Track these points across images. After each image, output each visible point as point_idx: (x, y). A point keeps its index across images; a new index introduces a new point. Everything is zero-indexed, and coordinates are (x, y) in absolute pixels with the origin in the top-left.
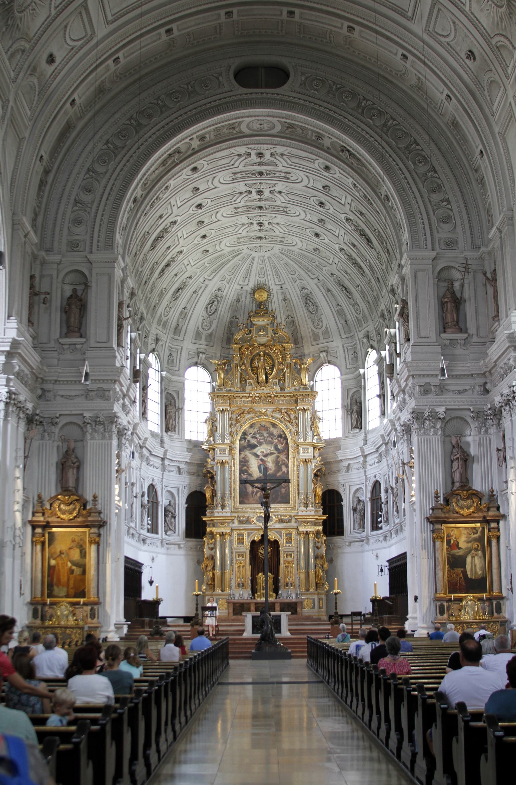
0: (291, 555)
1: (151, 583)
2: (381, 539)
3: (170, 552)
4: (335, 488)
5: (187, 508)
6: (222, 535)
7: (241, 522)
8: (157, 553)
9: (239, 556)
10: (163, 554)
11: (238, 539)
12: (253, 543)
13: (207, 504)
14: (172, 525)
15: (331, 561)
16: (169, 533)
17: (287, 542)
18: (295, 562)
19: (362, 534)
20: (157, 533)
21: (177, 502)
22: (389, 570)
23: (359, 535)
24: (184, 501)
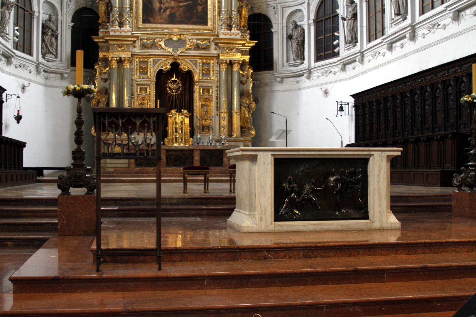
0: (208, 91)
1: (18, 118)
2: (337, 69)
3: (49, 82)
4: (262, 12)
5: (72, 27)
6: (120, 61)
7: (144, 46)
8: (28, 80)
9: (141, 89)
10: (39, 84)
11: (141, 68)
12: (160, 74)
13: (100, 21)
14: (52, 47)
15: (256, 100)
16: (48, 56)
17: (203, 74)
18: (214, 99)
19: (300, 67)
20: (31, 54)
21: (60, 18)
22: (356, 107)
23: (294, 69)
24: (70, 19)
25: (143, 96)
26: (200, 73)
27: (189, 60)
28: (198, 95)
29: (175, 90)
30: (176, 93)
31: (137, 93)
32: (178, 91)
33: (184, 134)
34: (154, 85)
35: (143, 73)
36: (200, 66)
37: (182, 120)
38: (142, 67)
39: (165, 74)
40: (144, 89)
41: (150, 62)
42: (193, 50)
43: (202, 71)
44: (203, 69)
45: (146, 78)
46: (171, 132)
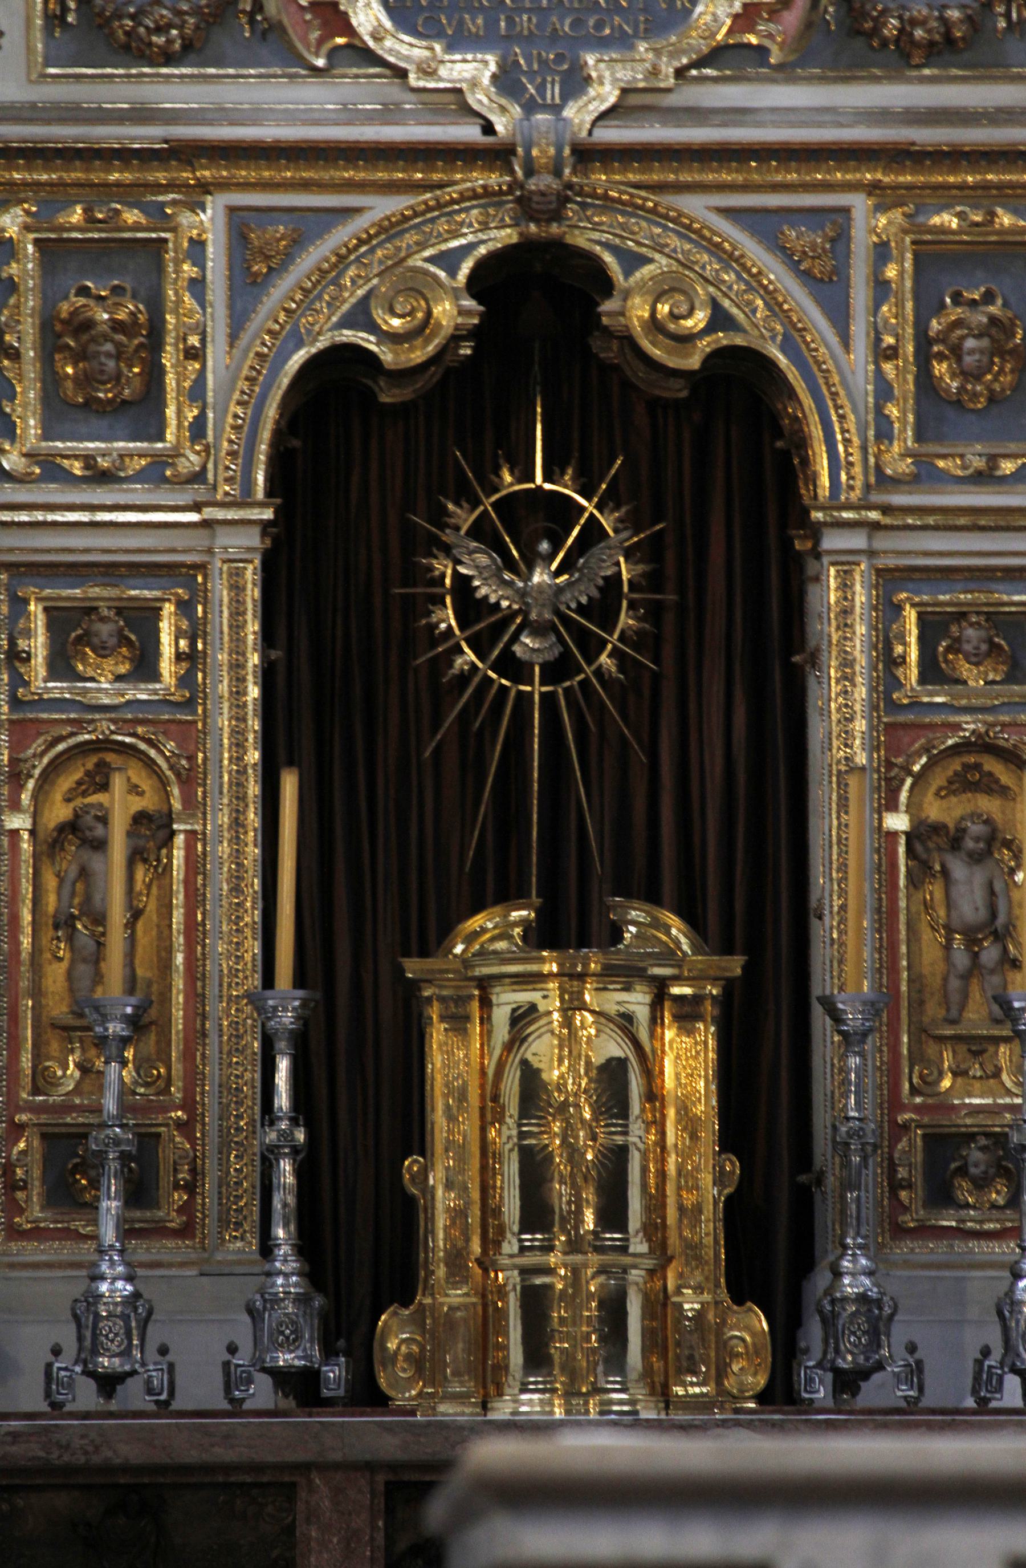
25: (105, 727)
26: (884, 391)
27: (726, 212)
28: (861, 692)
29: (539, 630)
30: (554, 672)
31: (18, 681)
32: (591, 647)
33: (639, 1246)
34: (251, 574)
35: (90, 405)
36: (881, 288)
37: (614, 1047)
38: (83, 326)
39: (403, 410)
40: (105, 630)
41: (198, 245)
42: (785, 72)
43: (924, 358)
44: (923, 341)
45: (140, 477)
46: (459, 1215)
